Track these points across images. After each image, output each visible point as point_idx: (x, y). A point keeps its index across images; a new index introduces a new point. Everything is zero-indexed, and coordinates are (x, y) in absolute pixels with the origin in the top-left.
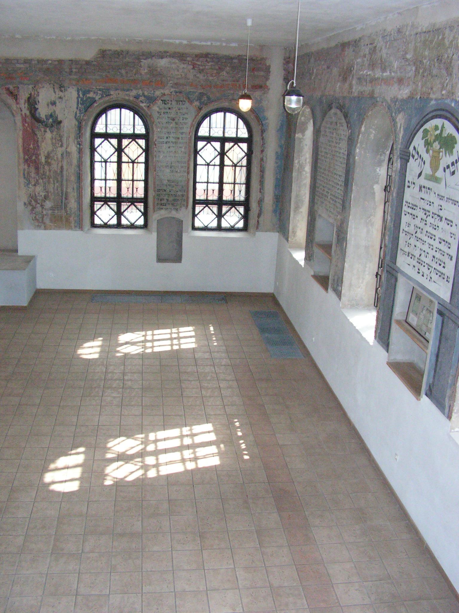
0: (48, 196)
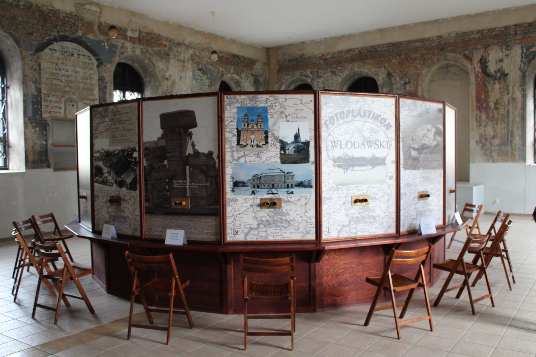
0: (496, 135)
